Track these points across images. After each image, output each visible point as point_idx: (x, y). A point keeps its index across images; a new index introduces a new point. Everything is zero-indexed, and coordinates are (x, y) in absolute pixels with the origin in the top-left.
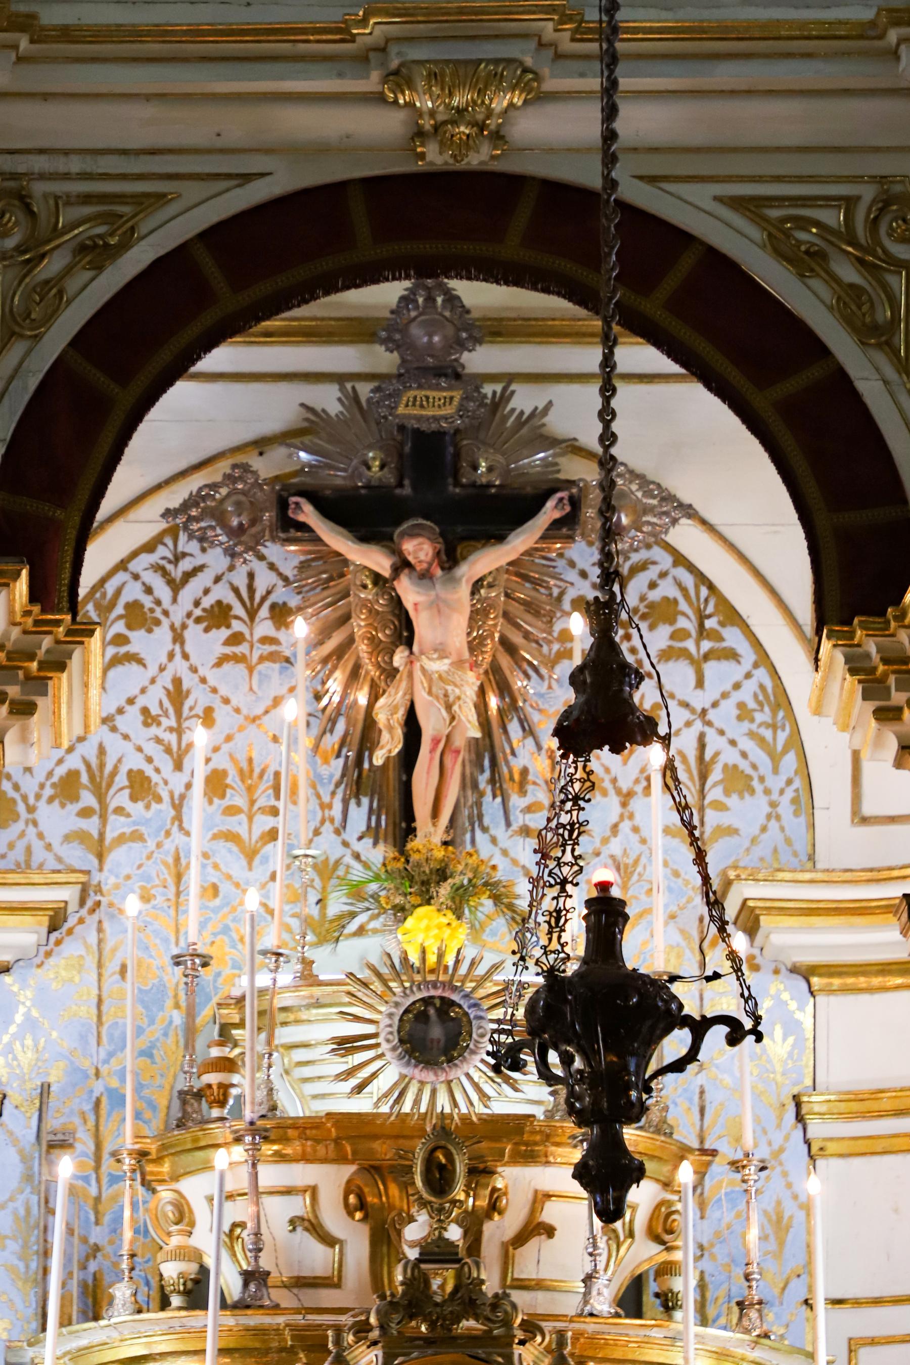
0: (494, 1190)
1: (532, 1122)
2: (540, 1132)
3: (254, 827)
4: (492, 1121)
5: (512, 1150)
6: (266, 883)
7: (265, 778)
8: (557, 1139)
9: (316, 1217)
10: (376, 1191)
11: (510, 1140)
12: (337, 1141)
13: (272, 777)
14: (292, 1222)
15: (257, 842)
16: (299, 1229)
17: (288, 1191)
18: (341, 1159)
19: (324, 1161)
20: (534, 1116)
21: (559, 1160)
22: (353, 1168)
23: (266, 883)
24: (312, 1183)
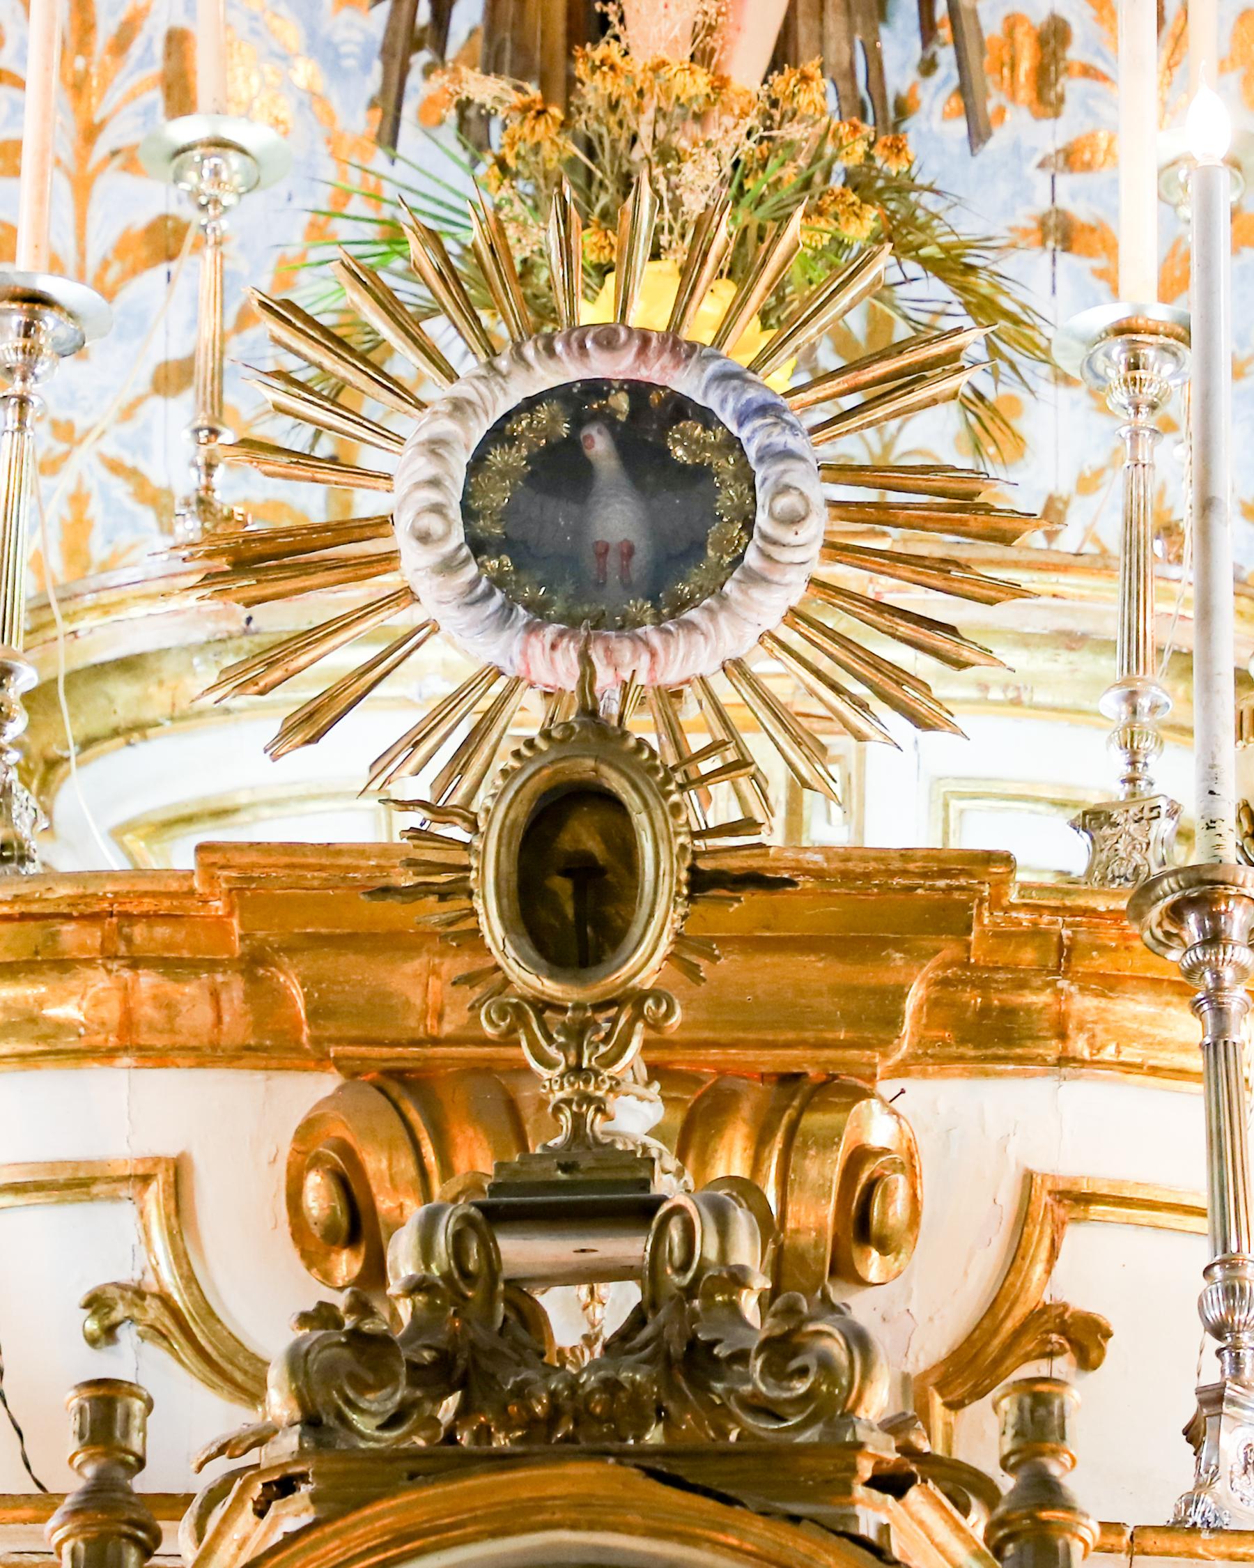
0: (860, 1155)
1: (1000, 884)
2: (1035, 933)
3: (95, 213)
4: (846, 876)
5: (932, 1004)
6: (139, 400)
7: (136, 50)
8: (1099, 962)
9: (190, 1279)
10: (406, 1165)
11: (918, 956)
12: (253, 963)
13: (159, 48)
14: (96, 1303)
15: (105, 265)
16: (127, 1334)
17: (75, 1184)
18: (269, 1048)
19: (208, 1054)
20: (1007, 859)
21: (1108, 1053)
22: (328, 1083)
23: (139, 400)
24: (172, 1151)
